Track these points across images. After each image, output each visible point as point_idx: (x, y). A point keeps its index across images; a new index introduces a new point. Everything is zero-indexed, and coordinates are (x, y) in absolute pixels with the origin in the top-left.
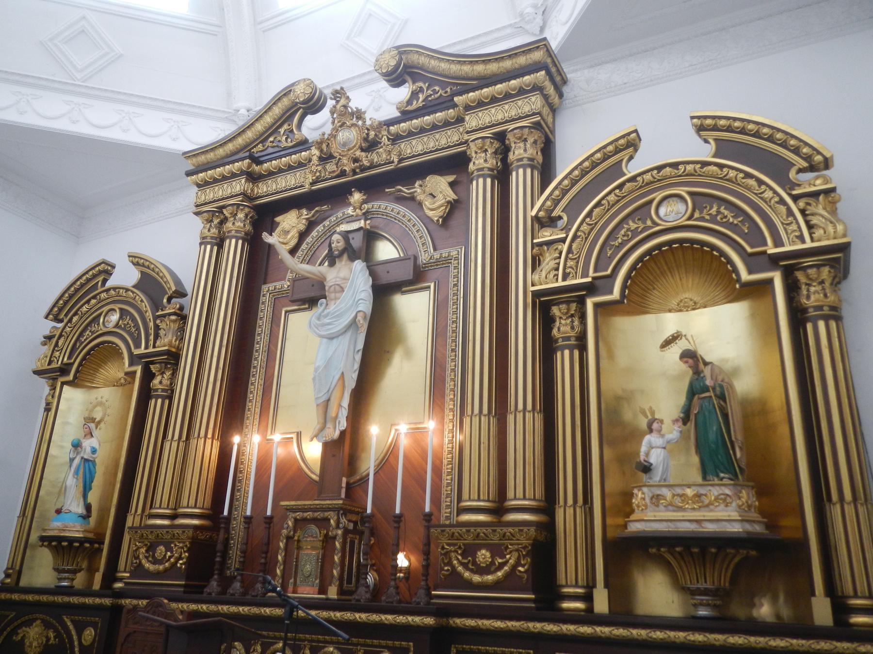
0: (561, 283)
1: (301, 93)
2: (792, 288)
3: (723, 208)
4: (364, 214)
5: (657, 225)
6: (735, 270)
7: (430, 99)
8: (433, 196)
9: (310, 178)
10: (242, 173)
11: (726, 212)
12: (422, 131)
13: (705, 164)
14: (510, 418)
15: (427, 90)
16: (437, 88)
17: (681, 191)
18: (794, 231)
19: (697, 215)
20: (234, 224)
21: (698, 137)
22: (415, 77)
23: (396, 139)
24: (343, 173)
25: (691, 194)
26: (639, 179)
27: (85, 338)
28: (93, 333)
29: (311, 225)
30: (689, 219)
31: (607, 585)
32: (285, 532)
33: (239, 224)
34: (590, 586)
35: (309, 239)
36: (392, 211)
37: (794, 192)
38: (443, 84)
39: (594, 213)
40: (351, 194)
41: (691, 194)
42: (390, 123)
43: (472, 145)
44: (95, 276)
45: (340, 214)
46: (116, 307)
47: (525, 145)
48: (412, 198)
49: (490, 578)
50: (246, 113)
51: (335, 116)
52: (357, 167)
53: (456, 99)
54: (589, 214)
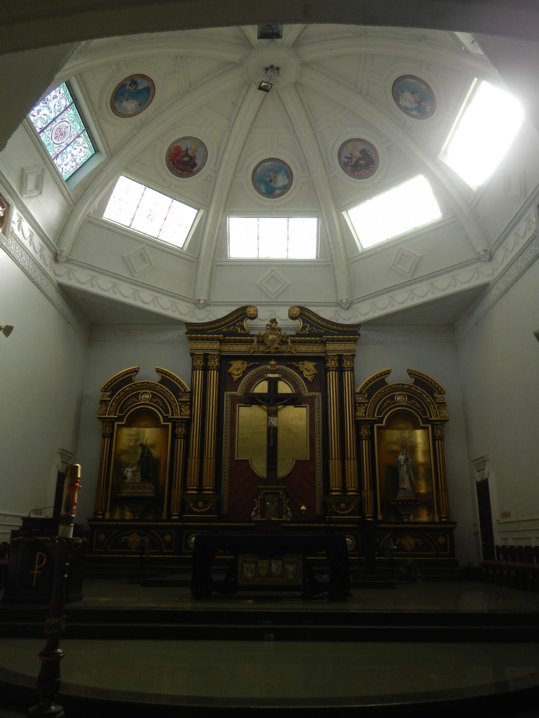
0: (367, 418)
1: (251, 311)
3: (416, 401)
4: (277, 370)
5: (396, 403)
6: (419, 422)
7: (311, 332)
8: (308, 370)
9: (252, 350)
10: (218, 339)
11: (417, 403)
12: (306, 342)
13: (412, 386)
14: (346, 462)
15: (309, 328)
16: (314, 328)
18: (435, 413)
19: (408, 402)
20: (215, 363)
21: (409, 376)
23: (293, 342)
24: (270, 352)
25: (407, 395)
26: (392, 386)
27: (129, 404)
28: (135, 402)
29: (249, 369)
30: (406, 403)
31: (381, 513)
32: (259, 497)
33: (216, 364)
35: (248, 375)
36: (289, 371)
37: (436, 401)
39: (377, 395)
41: (407, 395)
43: (330, 357)
44: (131, 373)
45: (263, 367)
47: (350, 362)
48: (298, 368)
49: (346, 512)
50: (203, 302)
51: (268, 326)
52: (276, 352)
53: (323, 336)
54: (376, 396)
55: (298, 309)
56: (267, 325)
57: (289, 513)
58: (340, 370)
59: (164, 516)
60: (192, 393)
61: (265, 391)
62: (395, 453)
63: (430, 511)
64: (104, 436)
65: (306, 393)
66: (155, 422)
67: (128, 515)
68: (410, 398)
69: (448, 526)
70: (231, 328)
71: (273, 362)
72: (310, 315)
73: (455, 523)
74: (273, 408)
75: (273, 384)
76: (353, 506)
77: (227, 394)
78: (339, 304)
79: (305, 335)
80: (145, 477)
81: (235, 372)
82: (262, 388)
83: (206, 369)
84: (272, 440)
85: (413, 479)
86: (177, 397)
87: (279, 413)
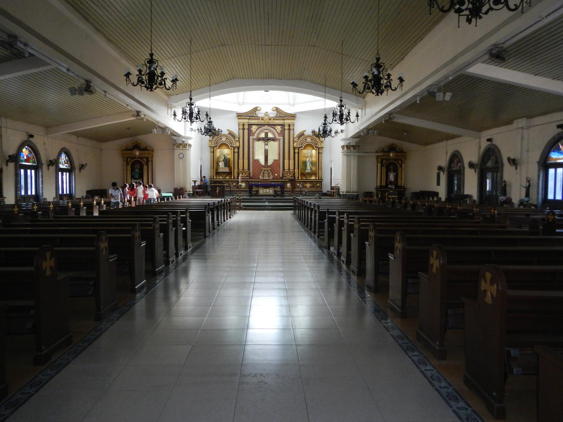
0: (298, 146)
1: (258, 109)
2: (319, 150)
10: (248, 119)
22: (277, 112)
23: (273, 119)
34: (299, 176)
38: (282, 115)
42: (273, 117)
55: (275, 108)
57: (272, 176)
58: (289, 130)
59: (233, 177)
60: (239, 138)
61: (264, 136)
62: (307, 157)
63: (316, 176)
64: (211, 152)
65: (277, 137)
67: (221, 178)
68: (312, 139)
69: (320, 180)
70: (252, 115)
71: (266, 126)
72: (279, 110)
73: (322, 180)
74: (266, 143)
75: (266, 134)
76: (291, 174)
77: (251, 137)
78: (289, 104)
80: (226, 165)
81: (253, 130)
82: (263, 135)
83: (243, 129)
84: (266, 154)
85: (311, 166)
86: (235, 139)
87: (269, 144)
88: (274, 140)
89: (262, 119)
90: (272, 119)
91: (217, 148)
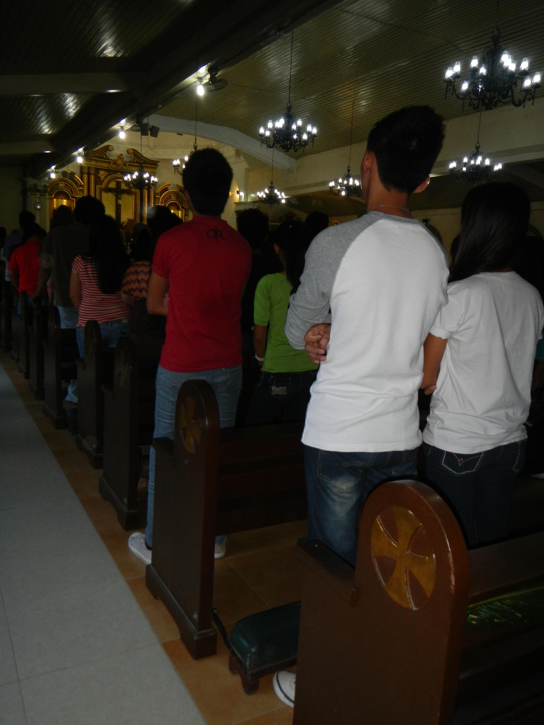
1: (111, 148)
10: (95, 160)
16: (139, 160)
17: (175, 195)
23: (129, 165)
24: (118, 169)
28: (57, 187)
29: (108, 175)
38: (140, 160)
40: (118, 172)
46: (63, 183)
56: (119, 156)
65: (133, 190)
66: (67, 198)
68: (177, 197)
71: (119, 173)
77: (98, 186)
79: (134, 163)
86: (78, 187)
88: (129, 192)
89: (115, 163)
90: (127, 164)
91: (53, 196)
